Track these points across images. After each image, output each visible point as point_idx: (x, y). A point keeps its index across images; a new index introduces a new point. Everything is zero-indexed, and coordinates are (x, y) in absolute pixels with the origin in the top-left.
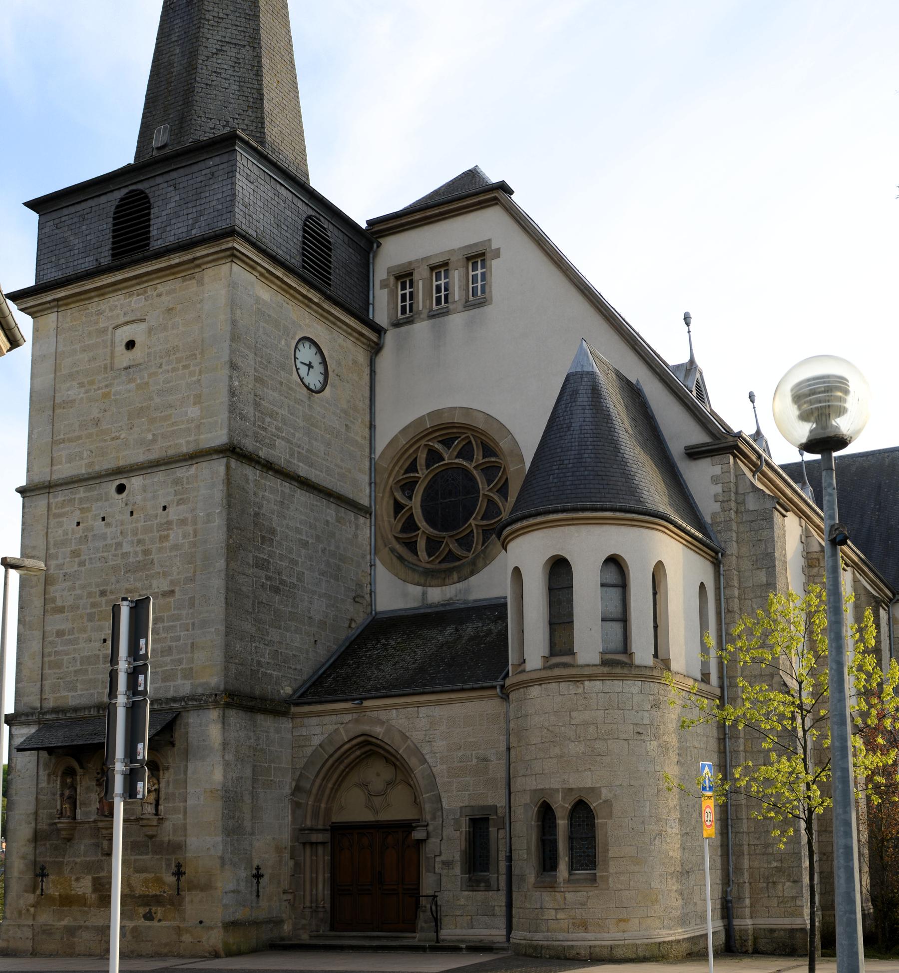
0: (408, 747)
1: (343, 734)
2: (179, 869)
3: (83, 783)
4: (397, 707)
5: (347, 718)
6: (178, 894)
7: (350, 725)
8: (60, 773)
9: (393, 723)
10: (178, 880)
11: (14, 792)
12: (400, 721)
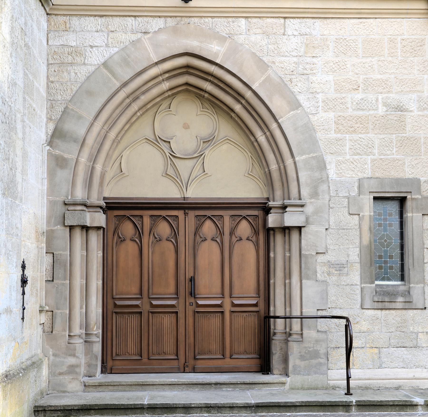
0: (268, 80)
1: (150, 49)
7: (162, 37)
9: (241, 39)
12: (253, 38)
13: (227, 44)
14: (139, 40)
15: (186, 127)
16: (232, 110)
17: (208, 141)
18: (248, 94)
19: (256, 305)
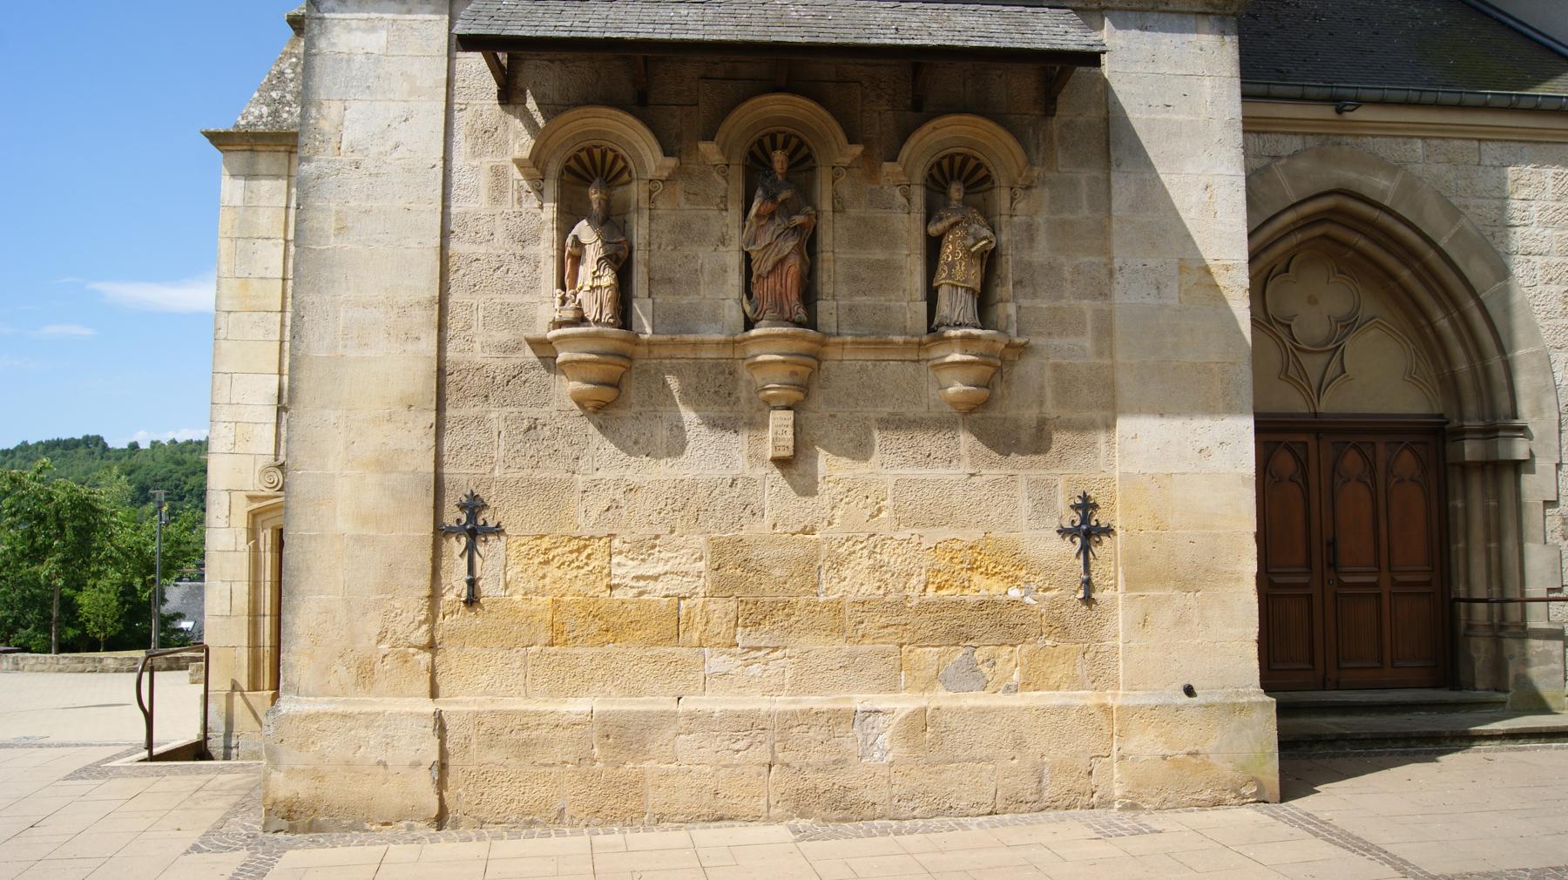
0: (1461, 233)
2: (1085, 519)
3: (662, 207)
4: (1424, 133)
5: (1291, 144)
6: (1088, 600)
8: (554, 168)
9: (1418, 169)
10: (1085, 550)
11: (330, 225)
12: (1434, 169)
13: (1399, 177)
14: (1267, 168)
15: (1313, 301)
16: (1393, 277)
17: (1349, 324)
18: (1431, 255)
19: (1428, 584)
